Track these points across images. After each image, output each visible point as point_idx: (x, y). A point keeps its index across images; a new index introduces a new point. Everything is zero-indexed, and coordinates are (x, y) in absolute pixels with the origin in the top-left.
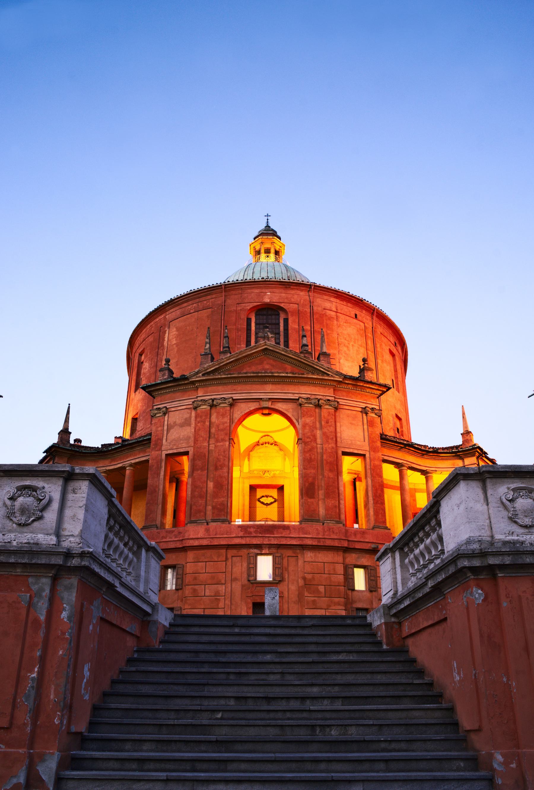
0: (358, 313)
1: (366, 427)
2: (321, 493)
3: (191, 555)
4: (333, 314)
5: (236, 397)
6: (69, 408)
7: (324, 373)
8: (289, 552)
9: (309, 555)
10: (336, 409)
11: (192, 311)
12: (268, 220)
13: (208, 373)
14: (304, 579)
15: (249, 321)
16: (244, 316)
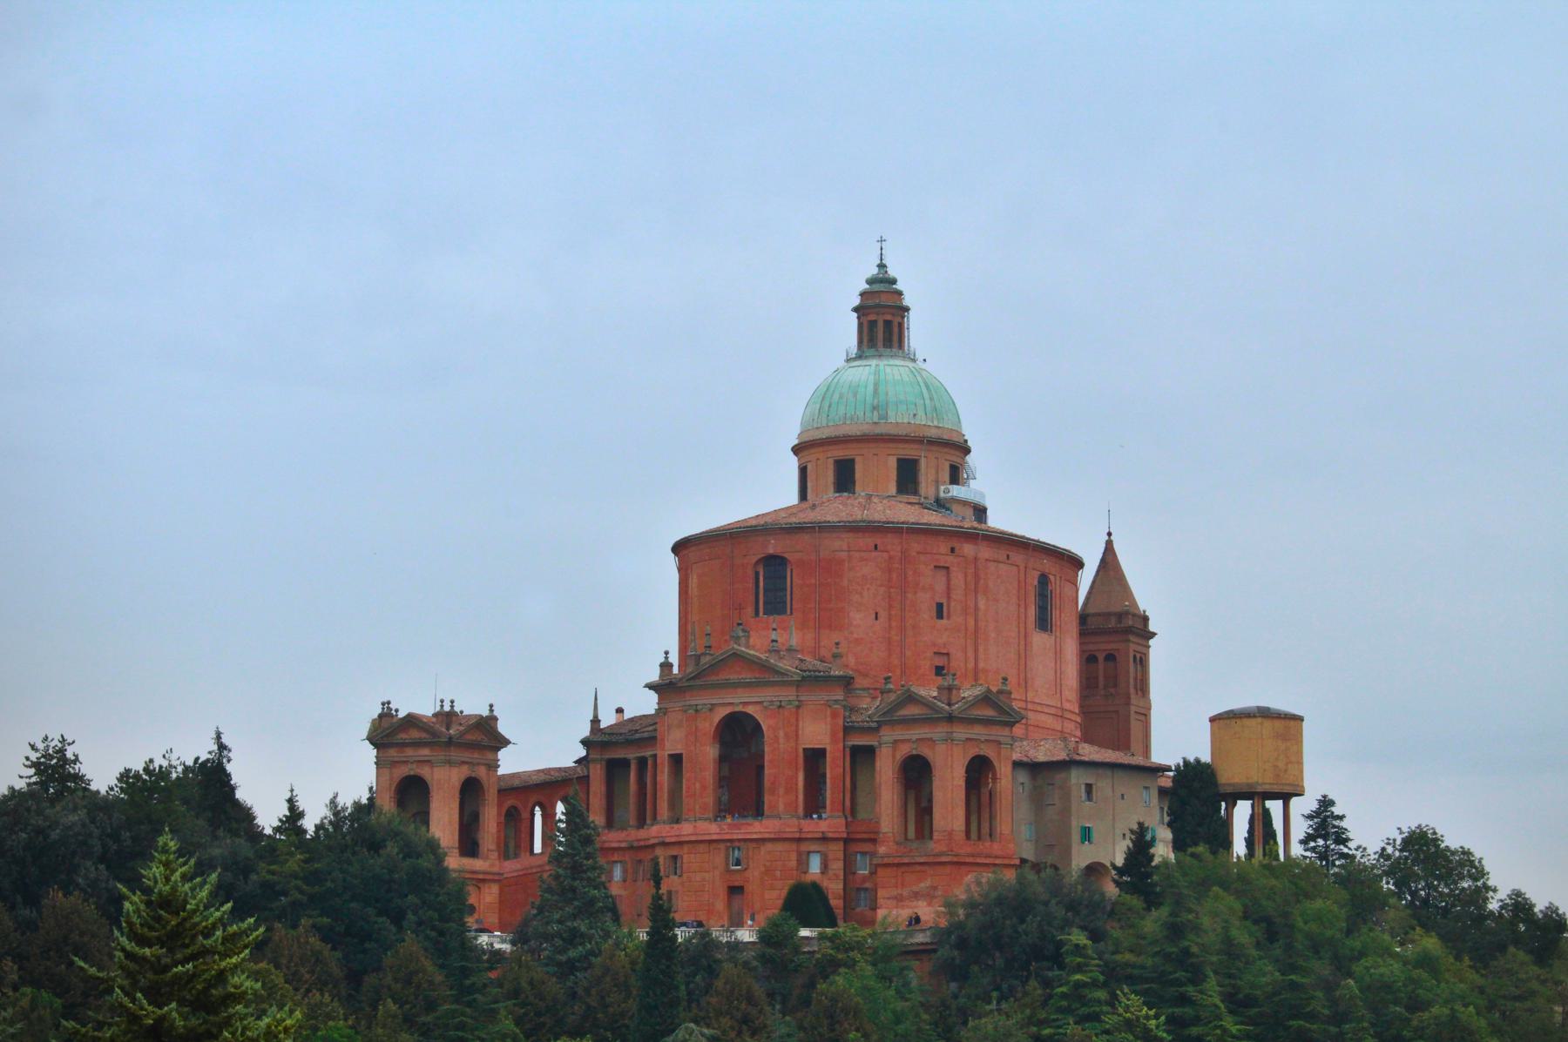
0: (878, 542)
1: (829, 719)
2: (781, 791)
3: (686, 848)
4: (843, 555)
5: (714, 702)
6: (596, 692)
7: (783, 674)
8: (754, 845)
9: (769, 846)
10: (798, 707)
11: (707, 558)
12: (881, 249)
13: (693, 678)
14: (765, 865)
15: (757, 574)
16: (750, 572)
